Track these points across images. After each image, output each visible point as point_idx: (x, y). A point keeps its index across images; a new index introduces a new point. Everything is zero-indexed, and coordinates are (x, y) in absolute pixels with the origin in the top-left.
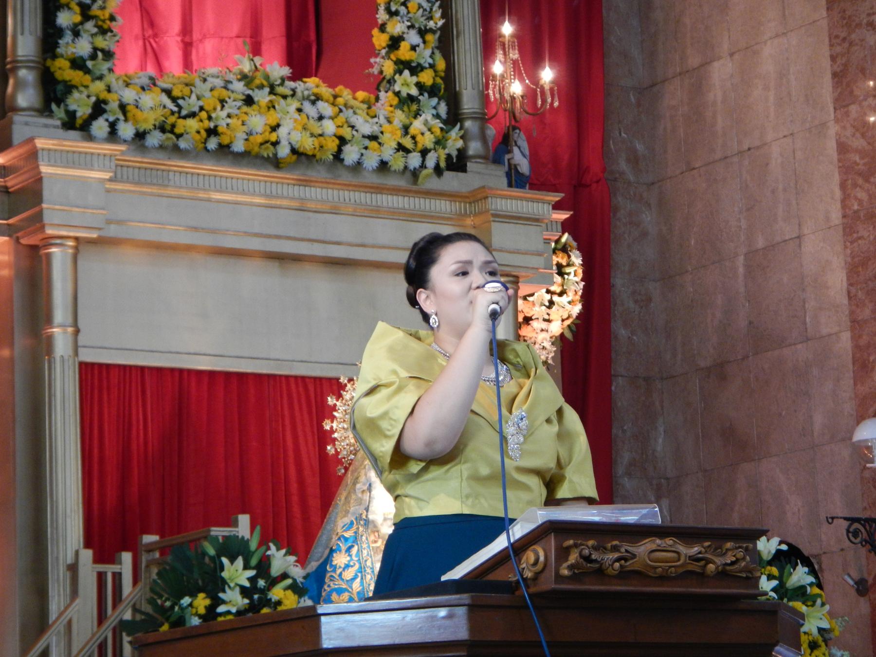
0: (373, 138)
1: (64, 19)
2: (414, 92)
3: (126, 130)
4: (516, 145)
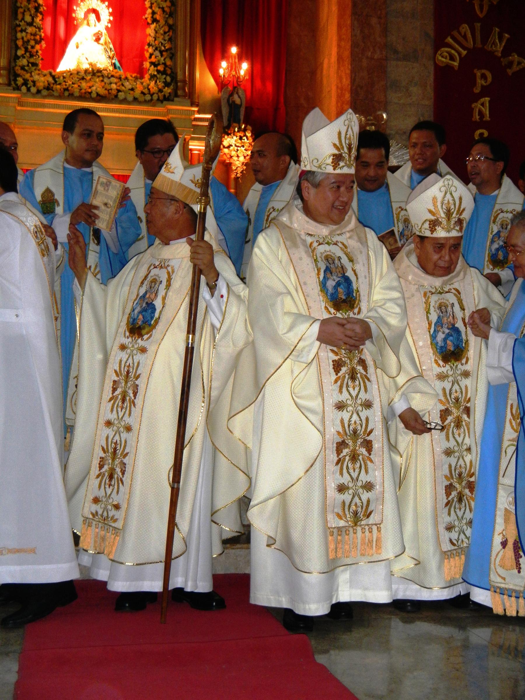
0: (132, 89)
1: (20, 53)
2: (156, 73)
3: (33, 90)
4: (237, 93)
